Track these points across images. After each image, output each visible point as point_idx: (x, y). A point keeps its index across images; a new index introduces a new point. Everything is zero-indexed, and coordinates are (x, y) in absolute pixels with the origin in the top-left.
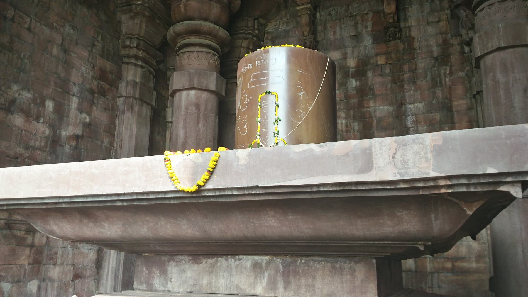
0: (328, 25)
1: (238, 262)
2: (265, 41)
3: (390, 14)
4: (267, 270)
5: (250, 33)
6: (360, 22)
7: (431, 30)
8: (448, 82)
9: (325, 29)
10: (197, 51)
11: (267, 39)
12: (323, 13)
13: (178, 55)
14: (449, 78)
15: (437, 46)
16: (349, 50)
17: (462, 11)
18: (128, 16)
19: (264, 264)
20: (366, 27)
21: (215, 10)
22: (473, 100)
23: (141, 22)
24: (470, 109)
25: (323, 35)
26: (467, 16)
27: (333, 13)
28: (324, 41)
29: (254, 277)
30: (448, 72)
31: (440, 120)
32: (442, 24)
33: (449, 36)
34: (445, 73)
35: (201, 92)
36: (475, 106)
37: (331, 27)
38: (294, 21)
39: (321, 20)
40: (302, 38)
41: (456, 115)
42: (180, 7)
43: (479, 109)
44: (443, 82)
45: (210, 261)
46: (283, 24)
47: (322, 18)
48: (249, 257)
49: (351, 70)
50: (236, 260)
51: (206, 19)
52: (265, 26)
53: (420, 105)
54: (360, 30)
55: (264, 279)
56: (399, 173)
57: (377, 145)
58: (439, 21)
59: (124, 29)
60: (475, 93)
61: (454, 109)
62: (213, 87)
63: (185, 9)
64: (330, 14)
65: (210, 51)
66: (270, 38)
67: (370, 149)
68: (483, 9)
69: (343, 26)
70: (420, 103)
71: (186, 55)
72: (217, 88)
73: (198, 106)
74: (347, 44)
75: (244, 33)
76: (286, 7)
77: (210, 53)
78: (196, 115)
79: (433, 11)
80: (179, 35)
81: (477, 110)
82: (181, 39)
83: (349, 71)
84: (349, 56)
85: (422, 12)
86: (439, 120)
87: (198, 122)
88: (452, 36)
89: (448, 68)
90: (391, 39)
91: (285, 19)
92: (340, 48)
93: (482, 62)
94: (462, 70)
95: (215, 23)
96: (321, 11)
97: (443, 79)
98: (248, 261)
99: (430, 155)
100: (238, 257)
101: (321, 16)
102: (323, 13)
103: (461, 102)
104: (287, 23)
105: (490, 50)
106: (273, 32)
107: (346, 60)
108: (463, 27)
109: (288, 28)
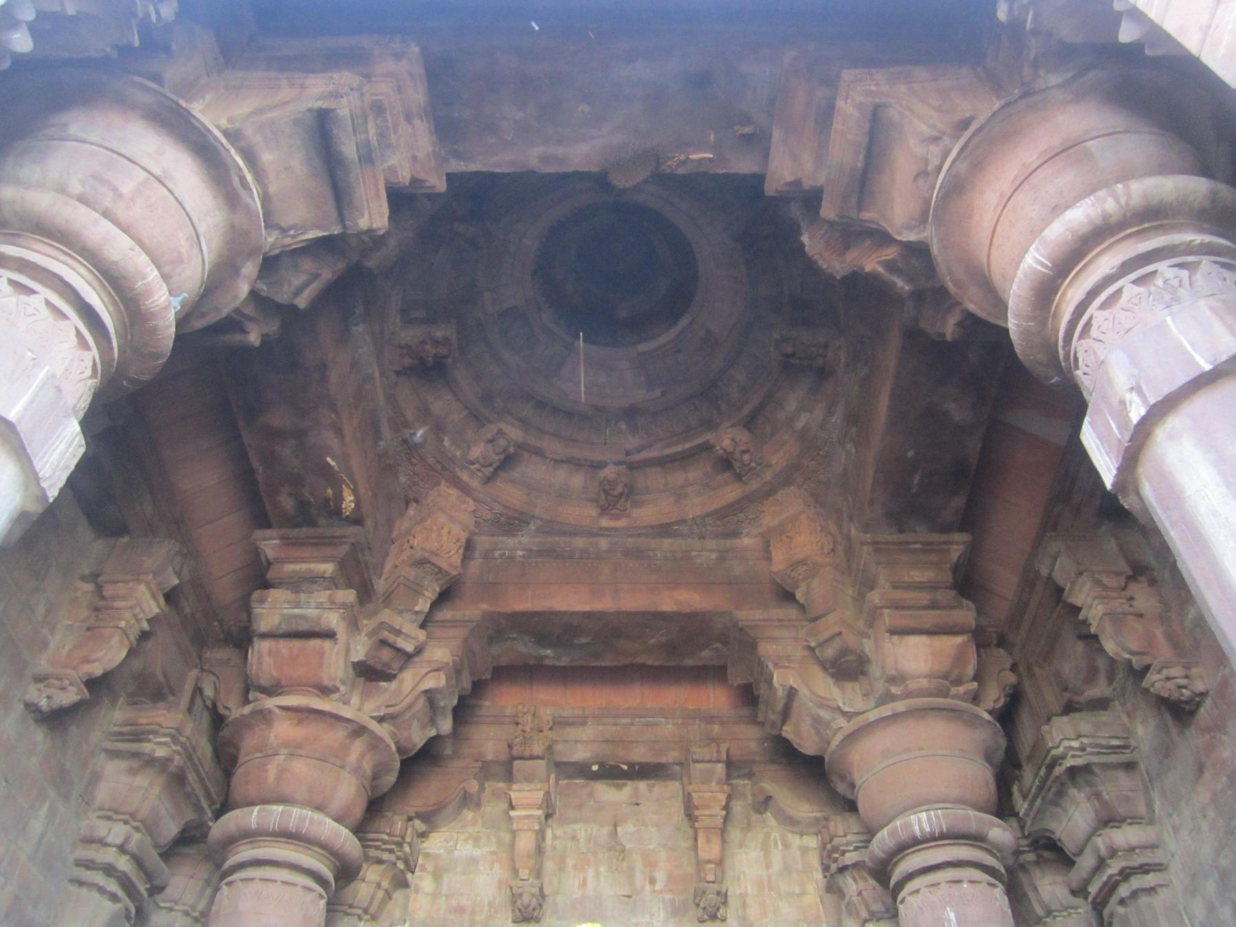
0: (570, 863)
2: (417, 873)
3: (709, 862)
5: (391, 851)
6: (639, 865)
9: (562, 868)
10: (284, 883)
11: (424, 869)
12: (559, 832)
13: (229, 884)
17: (850, 880)
18: (122, 764)
20: (653, 881)
21: (347, 791)
23: (151, 784)
26: (860, 894)
27: (582, 835)
28: (559, 898)
32: (807, 899)
37: (575, 867)
38: (493, 839)
39: (554, 848)
40: (513, 883)
42: (266, 771)
46: (466, 840)
47: (557, 842)
51: (319, 808)
52: (423, 835)
54: (638, 885)
58: (803, 893)
59: (103, 793)
63: (279, 778)
64: (574, 838)
66: (430, 869)
68: (917, 891)
71: (255, 887)
75: (378, 848)
76: (478, 805)
79: (787, 869)
80: (250, 836)
82: (249, 846)
85: (768, 866)
91: (470, 829)
96: (555, 826)
101: (555, 837)
102: (559, 832)
106: (439, 855)
108: (850, 913)
109: (477, 852)
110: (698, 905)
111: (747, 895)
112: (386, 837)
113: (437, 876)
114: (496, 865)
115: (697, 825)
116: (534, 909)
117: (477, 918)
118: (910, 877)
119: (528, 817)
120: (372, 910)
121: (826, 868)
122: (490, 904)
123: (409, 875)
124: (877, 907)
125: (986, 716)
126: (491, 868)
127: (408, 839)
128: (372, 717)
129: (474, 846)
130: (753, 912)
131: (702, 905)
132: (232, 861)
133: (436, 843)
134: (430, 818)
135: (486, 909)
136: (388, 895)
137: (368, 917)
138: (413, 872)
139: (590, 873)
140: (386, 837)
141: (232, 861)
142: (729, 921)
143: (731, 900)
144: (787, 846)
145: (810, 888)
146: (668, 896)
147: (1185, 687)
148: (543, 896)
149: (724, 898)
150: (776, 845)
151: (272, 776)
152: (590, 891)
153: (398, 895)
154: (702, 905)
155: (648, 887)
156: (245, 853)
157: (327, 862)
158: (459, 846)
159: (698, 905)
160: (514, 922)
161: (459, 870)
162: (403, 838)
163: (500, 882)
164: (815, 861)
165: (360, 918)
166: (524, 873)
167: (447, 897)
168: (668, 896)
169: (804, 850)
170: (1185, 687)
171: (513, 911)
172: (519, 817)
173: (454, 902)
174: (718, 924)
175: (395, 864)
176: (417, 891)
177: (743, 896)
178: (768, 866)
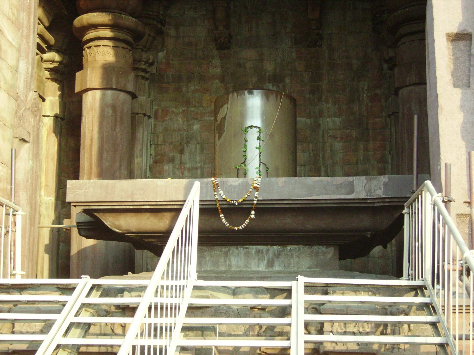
1: (245, 250)
2: (167, 27)
4: (267, 254)
5: (154, 19)
8: (365, 99)
13: (89, 48)
14: (367, 95)
19: (265, 251)
20: (285, 28)
22: (388, 120)
29: (257, 259)
30: (366, 88)
36: (389, 125)
41: (371, 132)
43: (393, 129)
44: (361, 98)
45: (225, 249)
48: (254, 247)
49: (267, 74)
50: (244, 249)
53: (338, 120)
55: (265, 260)
56: (367, 195)
57: (357, 181)
60: (391, 113)
62: (130, 88)
65: (125, 46)
67: (353, 182)
70: (337, 117)
71: (101, 49)
73: (114, 108)
77: (126, 49)
78: (114, 118)
81: (390, 129)
86: (354, 137)
87: (115, 126)
89: (366, 83)
93: (400, 92)
95: (131, 15)
98: (253, 249)
99: (382, 186)
100: (245, 247)
103: (377, 120)
105: (408, 84)
112: (151, 13)
113: (177, 29)
118: (402, 36)
132: (87, 37)
136: (154, 39)
138: (165, 26)
141: (87, 37)
146: (293, 35)
148: (230, 36)
156: (92, 34)
157: (130, 35)
160: (217, 49)
162: (159, 12)
165: (142, 50)
166: (221, 28)
171: (216, 45)
173: (186, 40)
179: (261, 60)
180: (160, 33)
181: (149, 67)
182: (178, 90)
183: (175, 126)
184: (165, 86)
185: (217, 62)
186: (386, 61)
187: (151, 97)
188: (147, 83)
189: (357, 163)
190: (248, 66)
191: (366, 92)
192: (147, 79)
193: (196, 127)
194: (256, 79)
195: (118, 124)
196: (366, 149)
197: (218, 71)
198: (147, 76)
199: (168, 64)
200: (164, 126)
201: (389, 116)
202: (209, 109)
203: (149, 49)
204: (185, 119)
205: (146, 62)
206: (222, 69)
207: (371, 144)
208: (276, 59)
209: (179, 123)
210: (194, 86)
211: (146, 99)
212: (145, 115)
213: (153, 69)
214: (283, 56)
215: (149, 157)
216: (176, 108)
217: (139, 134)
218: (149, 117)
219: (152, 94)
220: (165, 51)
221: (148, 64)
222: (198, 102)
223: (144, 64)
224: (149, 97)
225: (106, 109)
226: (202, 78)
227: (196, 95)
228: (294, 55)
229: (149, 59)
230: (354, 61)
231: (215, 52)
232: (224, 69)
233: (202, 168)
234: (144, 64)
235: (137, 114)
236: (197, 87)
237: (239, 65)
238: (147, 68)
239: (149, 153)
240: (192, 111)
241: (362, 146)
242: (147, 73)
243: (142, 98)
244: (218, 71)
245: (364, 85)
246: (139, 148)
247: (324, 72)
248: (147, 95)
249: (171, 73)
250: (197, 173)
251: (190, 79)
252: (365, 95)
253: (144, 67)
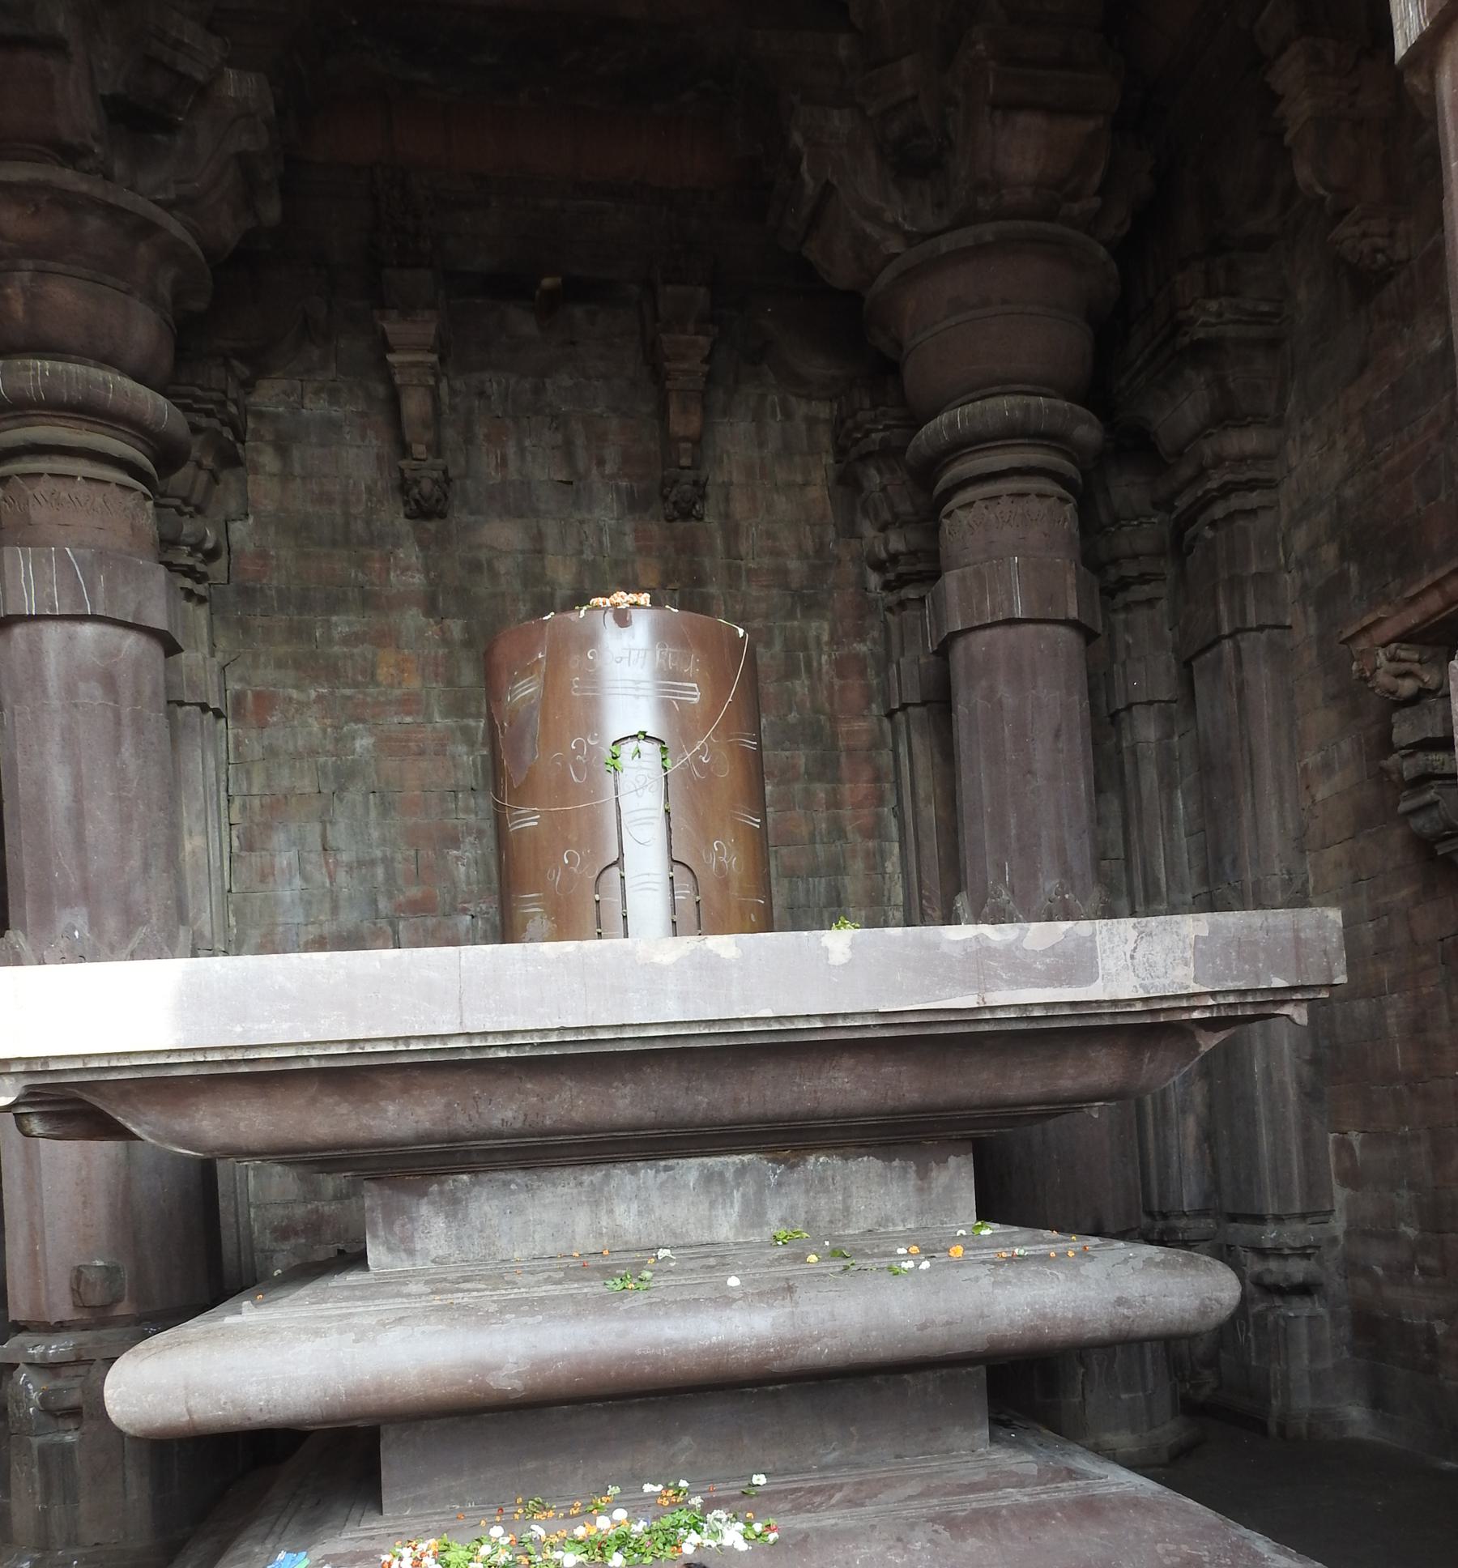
0: (480, 431)
2: (250, 444)
7: (782, 504)
8: (825, 668)
9: (469, 440)
11: (259, 437)
15: (799, 558)
16: (551, 529)
17: (873, 472)
20: (601, 462)
22: (886, 723)
24: (876, 745)
25: (462, 461)
26: (884, 489)
28: (468, 482)
30: (825, 638)
31: (806, 772)
33: (831, 533)
34: (818, 638)
35: (119, 631)
36: (890, 740)
39: (453, 408)
41: (843, 759)
43: (903, 750)
44: (815, 664)
47: (458, 400)
52: (248, 386)
54: (581, 466)
58: (806, 484)
61: (841, 743)
64: (482, 394)
66: (269, 437)
69: (527, 443)
72: (170, 625)
74: (542, 507)
83: (552, 595)
84: (550, 545)
85: (761, 445)
86: (802, 769)
88: (837, 534)
89: (826, 626)
90: (676, 514)
92: (521, 516)
94: (860, 636)
97: (814, 653)
101: (453, 392)
102: (458, 384)
103: (860, 725)
104: (334, 396)
106: (277, 417)
107: (542, 559)
108: (866, 514)
109: (336, 412)
110: (665, 498)
111: (731, 484)
113: (282, 450)
114: (370, 433)
115: (668, 384)
116: (438, 501)
117: (353, 511)
119: (413, 364)
120: (196, 498)
121: (840, 452)
122: (369, 490)
123: (239, 445)
124: (905, 507)
125: (1102, 252)
126: (363, 438)
127: (232, 394)
128: (155, 202)
129: (331, 404)
130: (739, 508)
131: (672, 498)
133: (270, 395)
134: (258, 363)
135: (364, 497)
136: (214, 478)
137: (191, 509)
139: (511, 451)
140: (199, 392)
142: (706, 519)
143: (709, 489)
144: (788, 415)
145: (818, 476)
146: (624, 484)
147: (1382, 251)
149: (700, 486)
150: (774, 415)
151: (18, 308)
152: (513, 475)
153: (226, 475)
154: (672, 498)
155: (594, 471)
158: (306, 401)
159: (665, 498)
160: (407, 516)
161: (314, 439)
163: (379, 458)
164: (825, 439)
165: (181, 513)
167: (303, 478)
168: (624, 484)
169: (812, 421)
170: (1382, 251)
171: (406, 503)
172: (402, 365)
174: (694, 523)
175: (220, 433)
176: (256, 470)
177: (727, 485)
178: (761, 445)
179: (540, 552)
180: (230, 459)
181: (202, 562)
182: (300, 632)
183: (300, 743)
184: (259, 621)
185: (409, 553)
186: (879, 566)
187: (219, 655)
188: (202, 613)
189: (813, 841)
190: (502, 566)
191: (826, 648)
192: (202, 600)
193: (363, 743)
194: (529, 606)
195: (128, 732)
196: (834, 803)
197: (417, 580)
198: (200, 589)
199: (262, 555)
200: (266, 743)
201: (890, 714)
202: (397, 692)
203: (199, 510)
204: (328, 721)
205: (196, 548)
206: (427, 575)
207: (846, 788)
208: (581, 552)
209: (310, 734)
210: (349, 623)
211: (204, 659)
212: (204, 708)
213: (218, 568)
214: (601, 543)
215: (225, 834)
216: (296, 687)
217: (191, 766)
218: (218, 715)
219: (222, 643)
220: (251, 520)
221: (200, 555)
222: (363, 672)
223: (190, 555)
224: (213, 655)
225: (82, 686)
226: (369, 600)
227: (355, 651)
228: (629, 542)
229: (204, 538)
230: (793, 564)
231: (403, 525)
232: (432, 574)
233: (387, 862)
234: (190, 555)
235: (181, 704)
236: (357, 628)
237: (475, 567)
238: (201, 567)
239: (224, 820)
240: (349, 698)
241: (822, 795)
242: (199, 581)
243: (193, 658)
244: (416, 580)
245: (820, 628)
246: (198, 805)
247: (713, 590)
248: (206, 651)
249: (275, 583)
250: (373, 876)
251: (335, 604)
252: (824, 658)
253: (190, 562)
